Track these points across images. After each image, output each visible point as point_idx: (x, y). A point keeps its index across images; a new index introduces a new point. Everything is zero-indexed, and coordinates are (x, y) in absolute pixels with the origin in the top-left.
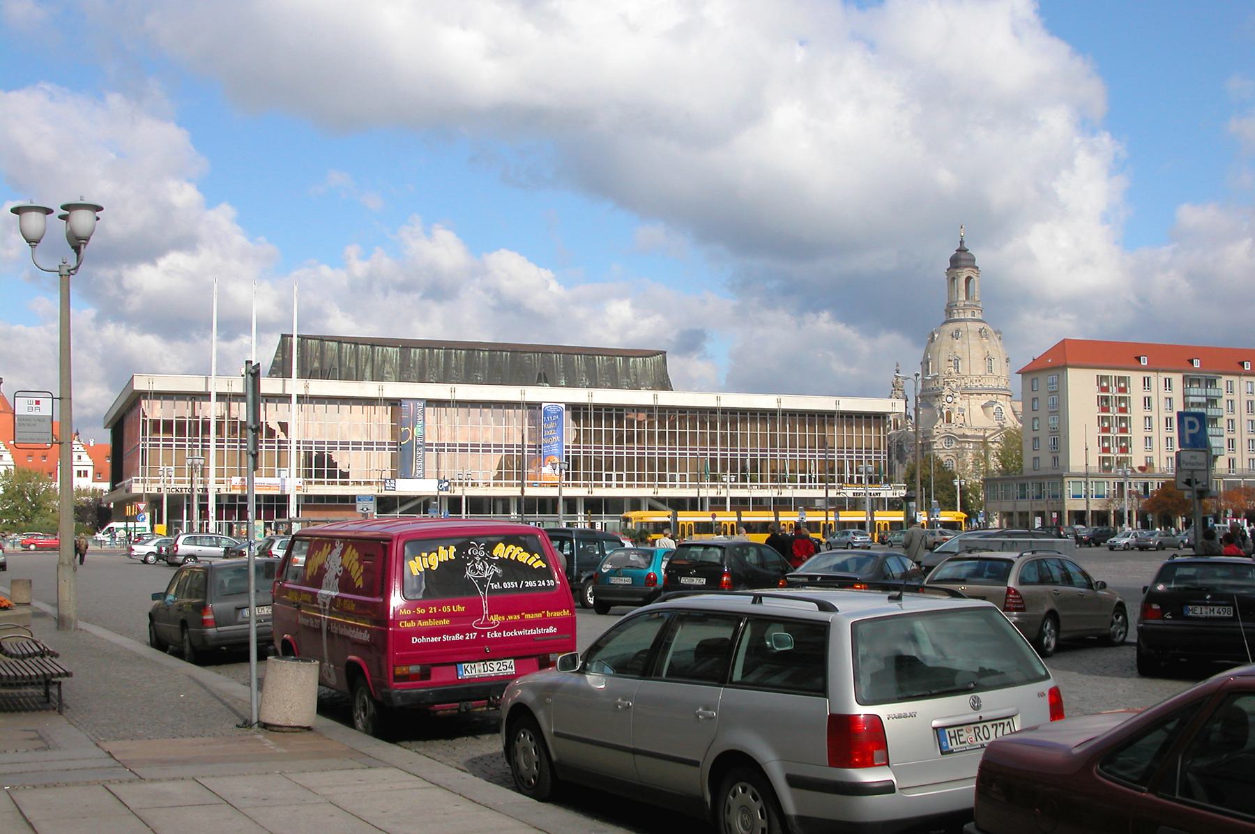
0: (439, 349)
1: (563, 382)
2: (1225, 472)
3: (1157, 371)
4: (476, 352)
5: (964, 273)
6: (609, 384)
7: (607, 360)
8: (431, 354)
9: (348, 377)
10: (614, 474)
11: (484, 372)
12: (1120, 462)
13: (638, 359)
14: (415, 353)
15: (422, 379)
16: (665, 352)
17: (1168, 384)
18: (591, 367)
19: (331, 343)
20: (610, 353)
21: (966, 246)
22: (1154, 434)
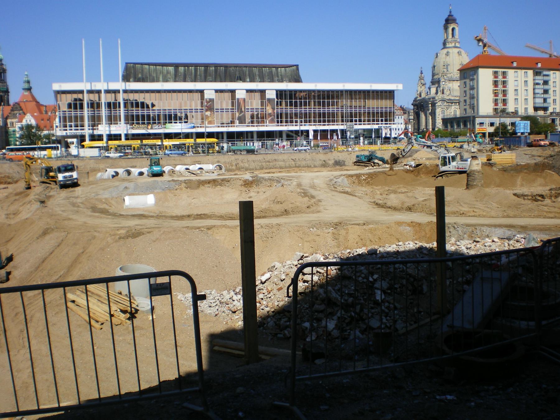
0: (191, 67)
1: (248, 80)
4: (209, 68)
6: (269, 80)
7: (268, 70)
8: (188, 69)
11: (212, 77)
12: (503, 111)
13: (282, 69)
14: (181, 69)
15: (185, 80)
16: (297, 66)
19: (145, 66)
20: (270, 66)
21: (452, 13)
22: (519, 97)
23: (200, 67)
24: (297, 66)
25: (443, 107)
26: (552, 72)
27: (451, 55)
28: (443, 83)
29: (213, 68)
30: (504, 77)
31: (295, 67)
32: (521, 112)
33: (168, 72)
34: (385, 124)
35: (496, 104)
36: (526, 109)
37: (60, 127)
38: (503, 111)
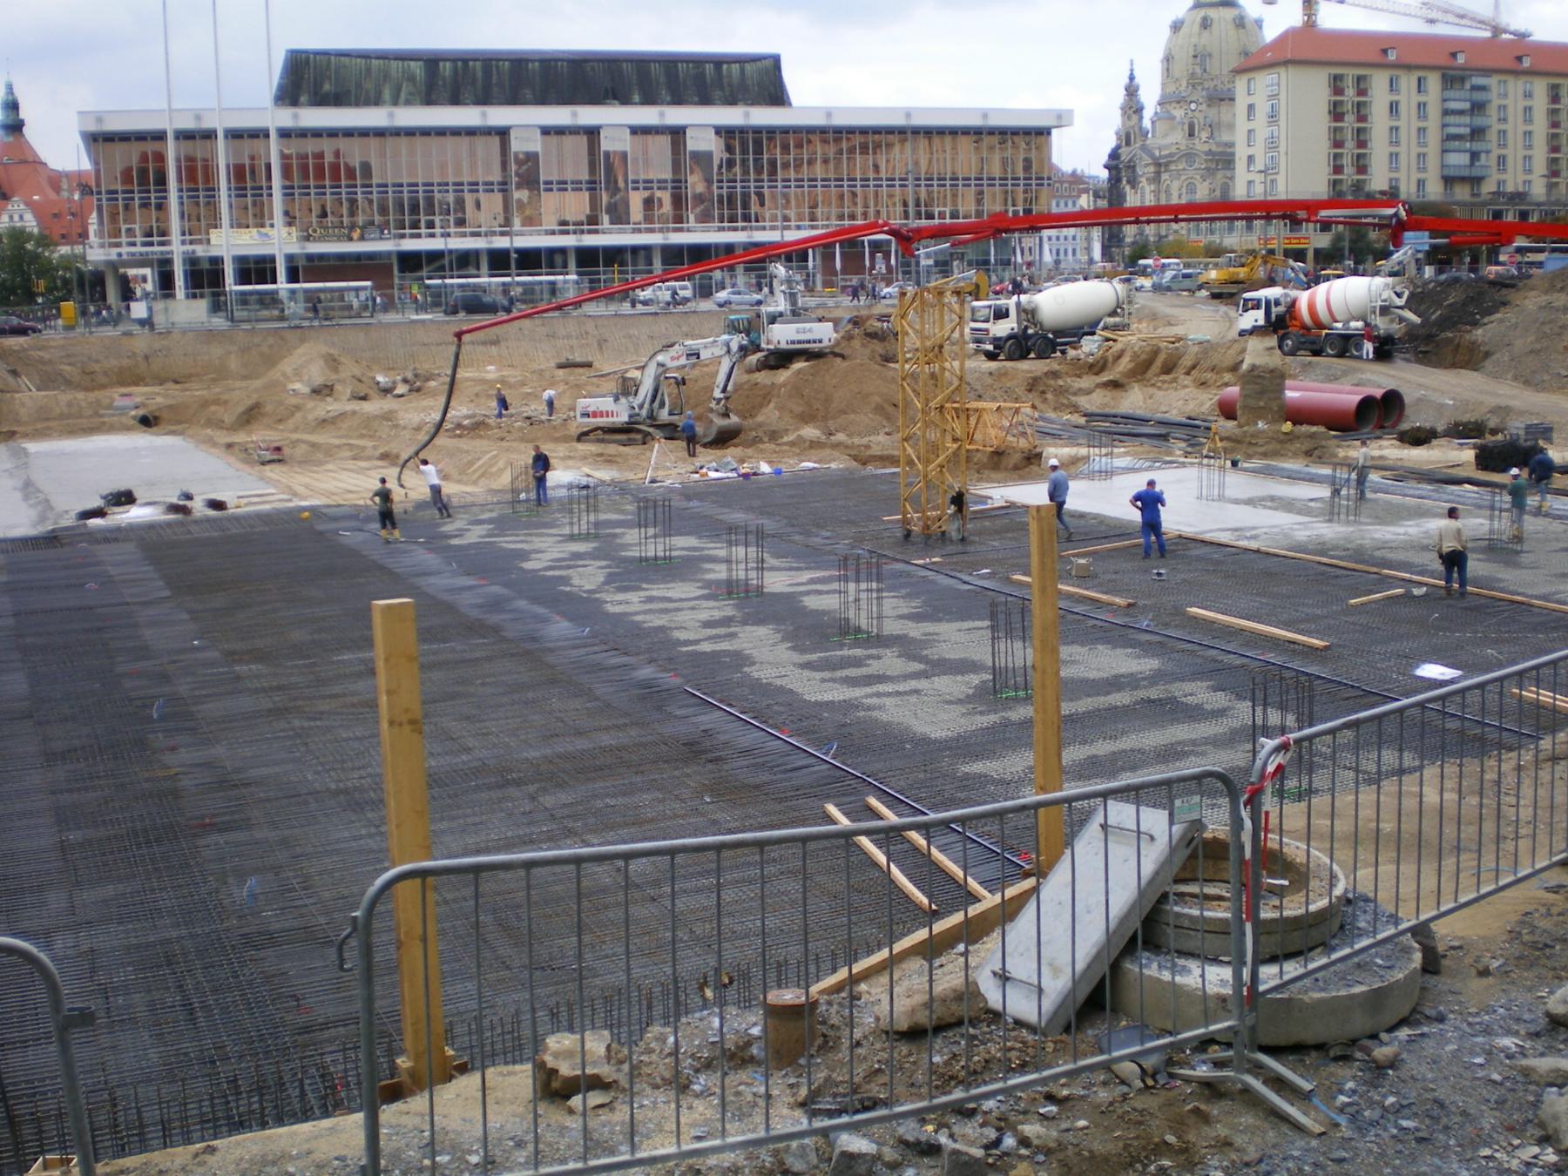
1: (636, 98)
2: (1543, 199)
12: (1358, 187)
15: (455, 101)
22: (1402, 150)
26: (1492, 81)
27: (1215, 27)
28: (1193, 106)
32: (1407, 190)
33: (411, 78)
35: (1338, 169)
36: (1421, 184)
38: (1358, 187)
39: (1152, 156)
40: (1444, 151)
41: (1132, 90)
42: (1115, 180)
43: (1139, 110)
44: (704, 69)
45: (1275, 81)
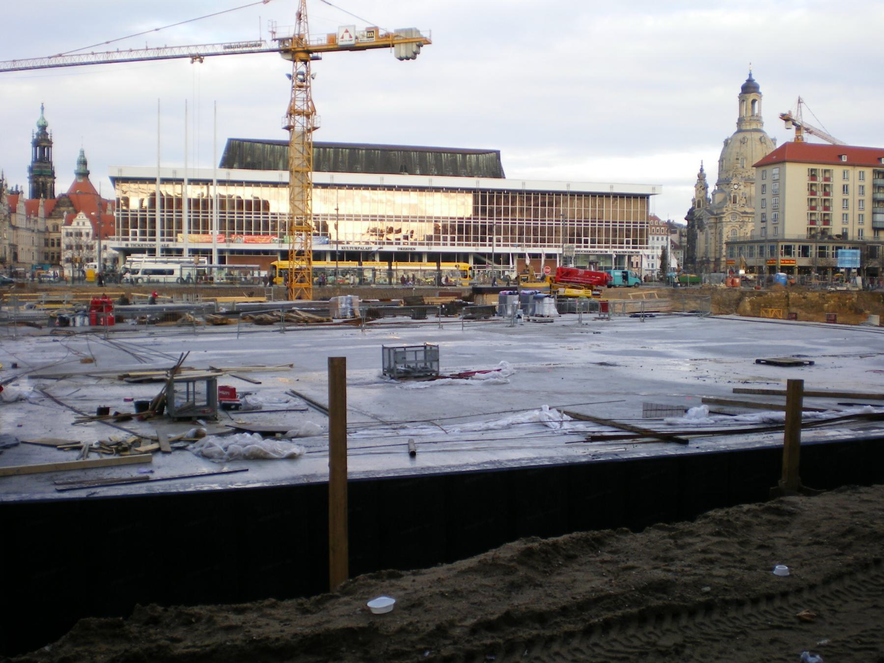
0: (330, 148)
1: (418, 172)
3: (854, 165)
5: (752, 97)
6: (451, 173)
8: (325, 151)
9: (269, 168)
10: (449, 236)
11: (362, 166)
12: (824, 232)
13: (472, 156)
17: (862, 177)
18: (438, 160)
19: (258, 144)
21: (753, 77)
22: (849, 212)
23: (343, 148)
24: (498, 153)
25: (734, 224)
27: (749, 143)
28: (736, 187)
29: (364, 151)
30: (827, 179)
31: (492, 155)
32: (852, 235)
34: (633, 248)
35: (812, 222)
36: (861, 232)
37: (118, 235)
38: (824, 232)
39: (712, 214)
40: (874, 213)
41: (701, 176)
42: (691, 226)
43: (705, 187)
44: (456, 157)
45: (777, 172)
